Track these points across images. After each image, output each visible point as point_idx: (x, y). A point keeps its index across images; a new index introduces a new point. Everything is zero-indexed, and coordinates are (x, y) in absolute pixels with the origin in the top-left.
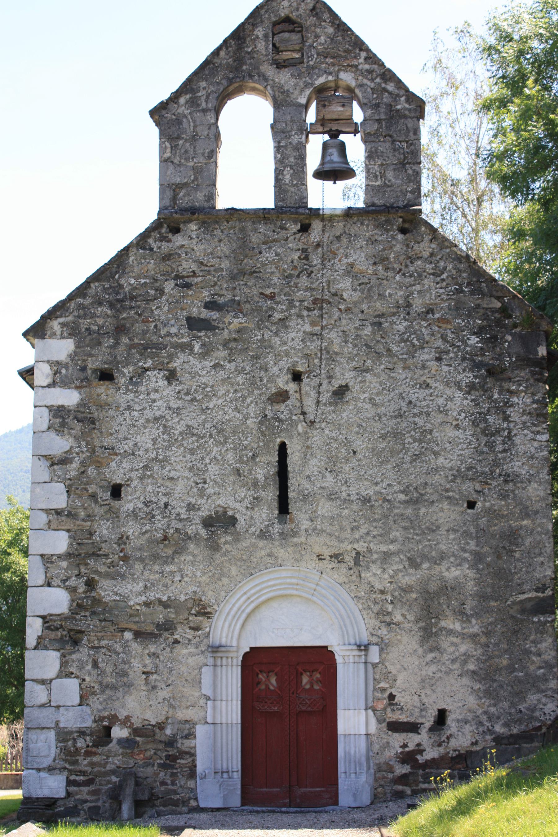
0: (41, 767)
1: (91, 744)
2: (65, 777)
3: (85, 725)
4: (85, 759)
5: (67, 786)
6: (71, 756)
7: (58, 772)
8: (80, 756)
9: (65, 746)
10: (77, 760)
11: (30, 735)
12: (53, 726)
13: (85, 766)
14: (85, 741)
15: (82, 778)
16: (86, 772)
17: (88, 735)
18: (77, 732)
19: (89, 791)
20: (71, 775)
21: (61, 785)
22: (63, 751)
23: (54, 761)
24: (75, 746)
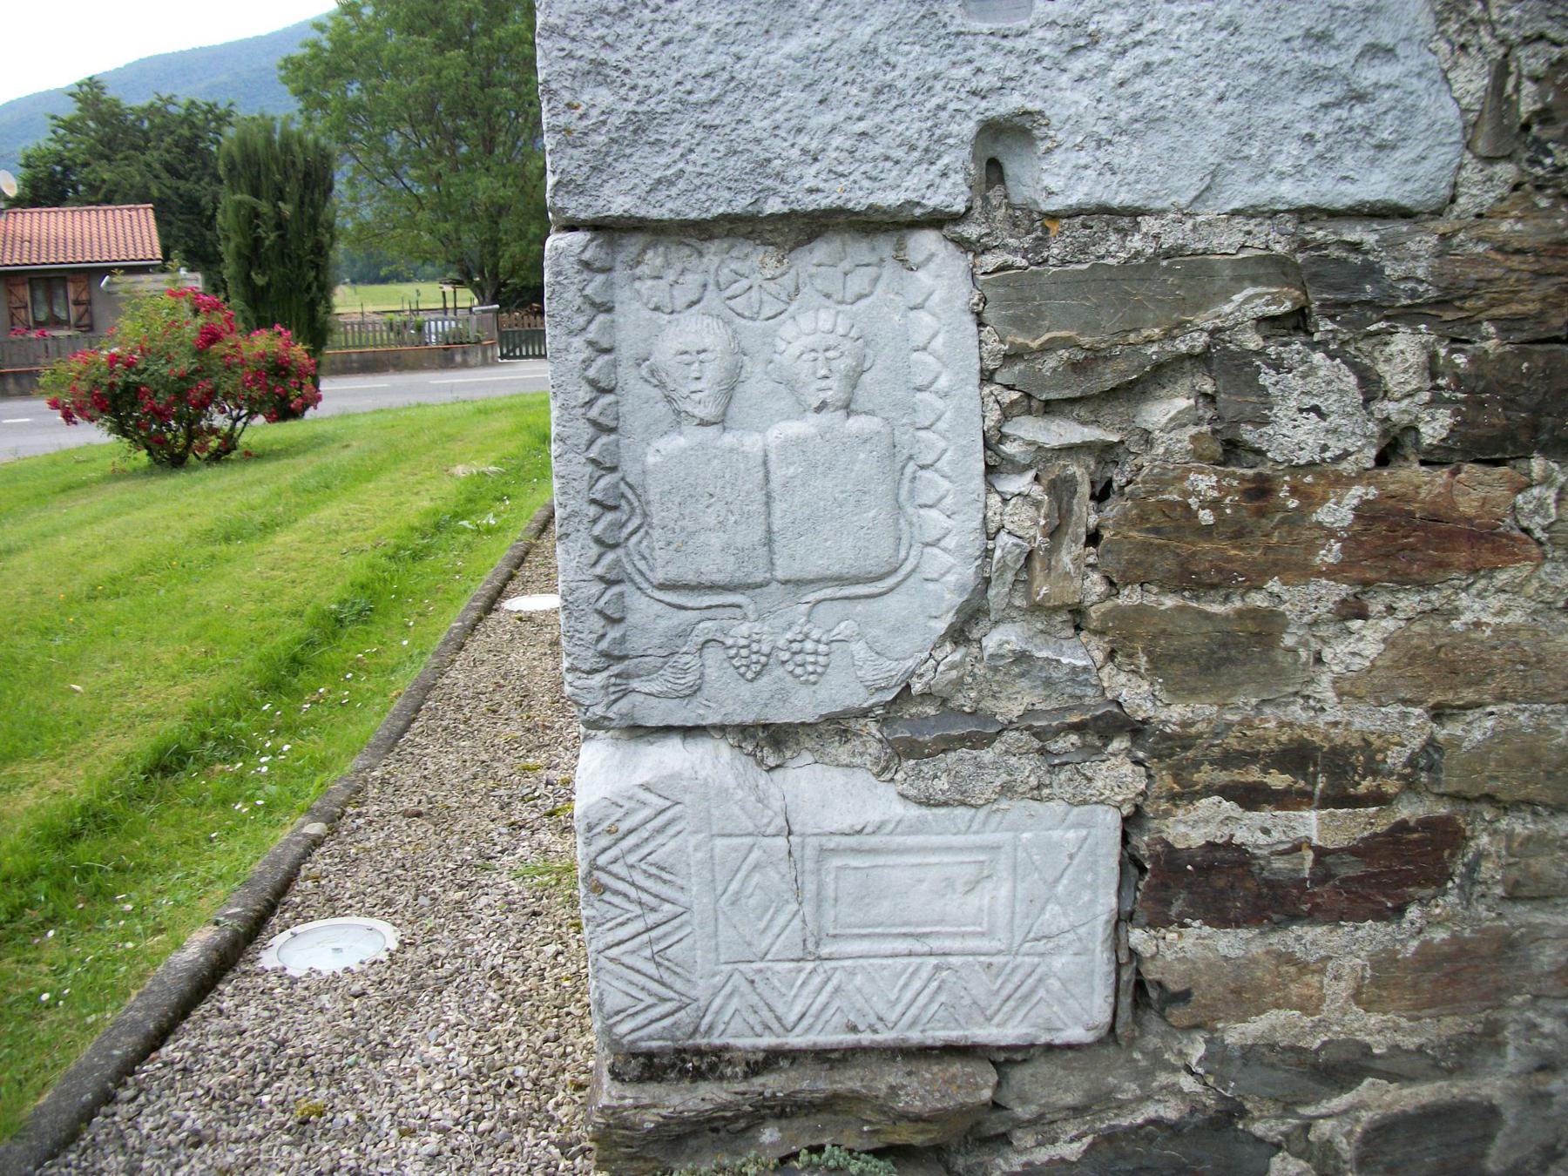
0: (802, 707)
1: (1435, 428)
2: (1108, 822)
3: (1376, 186)
4: (1353, 610)
5: (1123, 920)
6: (1187, 580)
7: (1028, 769)
8: (1303, 571)
9: (1105, 453)
10: (1266, 626)
11: (632, 320)
12: (951, 194)
13: (1346, 690)
14: (1371, 386)
15: (1310, 824)
16: (1369, 755)
17: (1411, 315)
18: (1273, 268)
19: (1384, 963)
20: (1187, 795)
21: (1053, 917)
22: (1086, 515)
23: (958, 634)
24: (1233, 450)
